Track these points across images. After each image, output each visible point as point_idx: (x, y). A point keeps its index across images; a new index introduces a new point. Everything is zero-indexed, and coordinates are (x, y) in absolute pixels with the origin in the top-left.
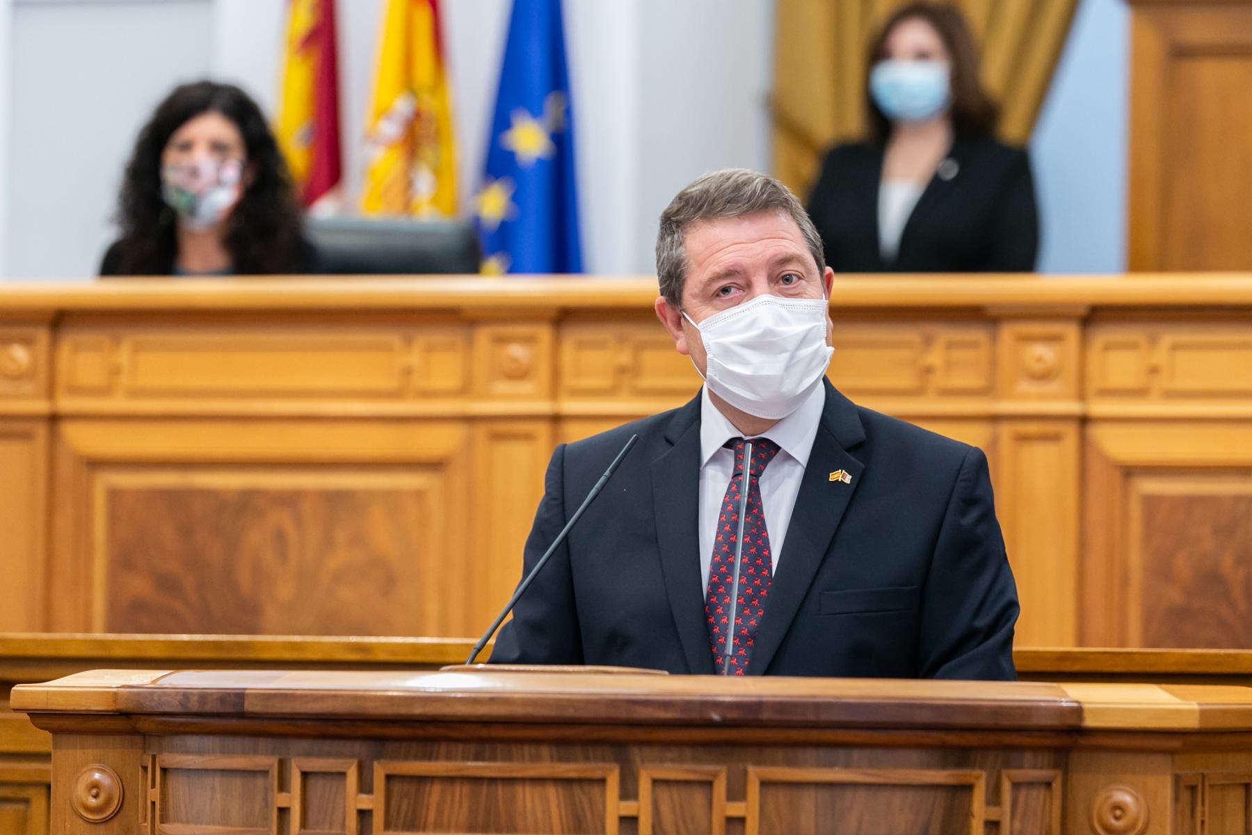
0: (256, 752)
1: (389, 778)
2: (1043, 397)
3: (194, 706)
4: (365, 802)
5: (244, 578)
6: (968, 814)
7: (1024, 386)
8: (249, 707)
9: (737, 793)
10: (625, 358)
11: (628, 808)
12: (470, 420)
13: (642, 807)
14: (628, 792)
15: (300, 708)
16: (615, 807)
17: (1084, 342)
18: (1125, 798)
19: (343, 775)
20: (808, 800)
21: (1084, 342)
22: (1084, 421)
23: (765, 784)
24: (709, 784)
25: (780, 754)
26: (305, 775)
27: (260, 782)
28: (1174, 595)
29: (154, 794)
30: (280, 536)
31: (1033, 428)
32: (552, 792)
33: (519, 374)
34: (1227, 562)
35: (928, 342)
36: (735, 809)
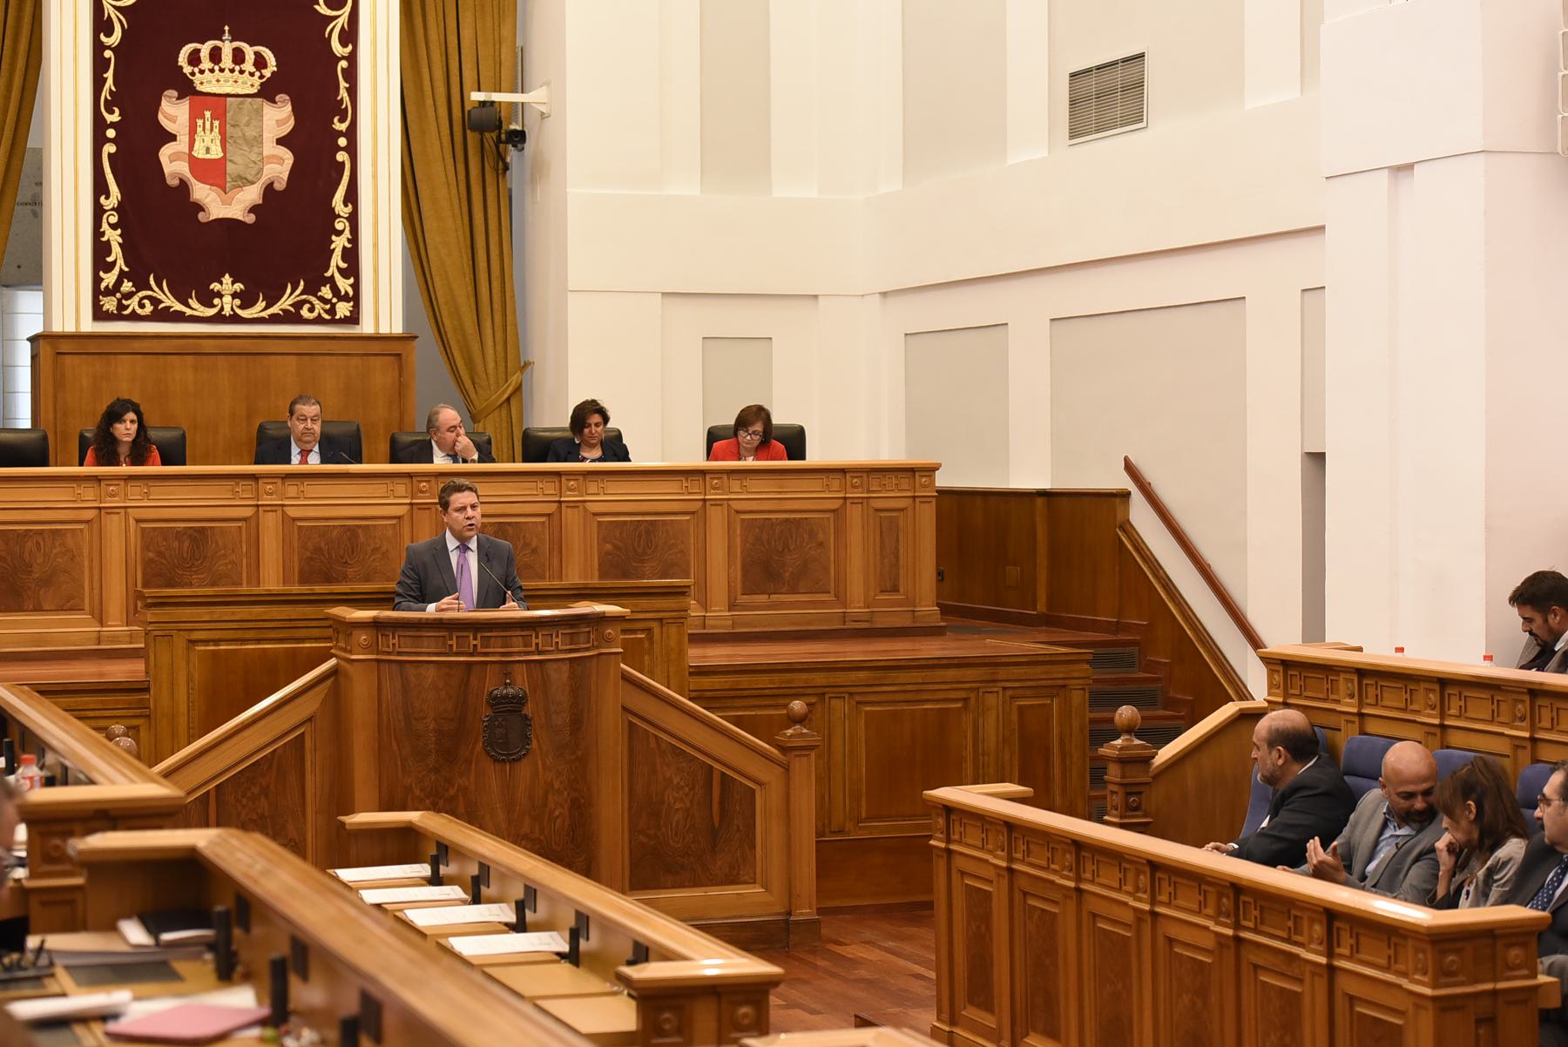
0: (439, 632)
1: (481, 637)
2: (271, 500)
3: (424, 621)
4: (475, 642)
5: (26, 555)
6: (590, 637)
7: (265, 496)
8: (444, 622)
9: (557, 637)
10: (146, 491)
11: (537, 641)
12: (100, 508)
13: (540, 641)
14: (537, 637)
15: (461, 622)
16: (534, 641)
17: (283, 484)
18: (609, 631)
19: (469, 637)
20: (568, 636)
21: (283, 484)
22: (283, 505)
23: (562, 634)
24: (551, 635)
25: (564, 627)
26: (457, 637)
27: (441, 638)
28: (309, 554)
29: (396, 641)
30: (38, 543)
31: (269, 508)
32: (520, 638)
33: (114, 496)
34: (323, 545)
35: (238, 484)
36: (557, 640)
